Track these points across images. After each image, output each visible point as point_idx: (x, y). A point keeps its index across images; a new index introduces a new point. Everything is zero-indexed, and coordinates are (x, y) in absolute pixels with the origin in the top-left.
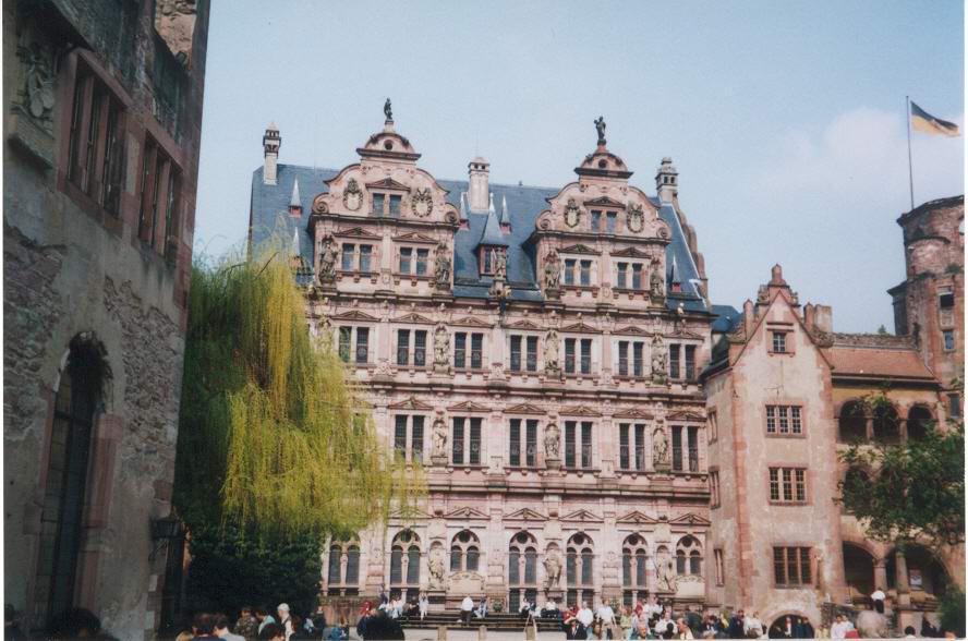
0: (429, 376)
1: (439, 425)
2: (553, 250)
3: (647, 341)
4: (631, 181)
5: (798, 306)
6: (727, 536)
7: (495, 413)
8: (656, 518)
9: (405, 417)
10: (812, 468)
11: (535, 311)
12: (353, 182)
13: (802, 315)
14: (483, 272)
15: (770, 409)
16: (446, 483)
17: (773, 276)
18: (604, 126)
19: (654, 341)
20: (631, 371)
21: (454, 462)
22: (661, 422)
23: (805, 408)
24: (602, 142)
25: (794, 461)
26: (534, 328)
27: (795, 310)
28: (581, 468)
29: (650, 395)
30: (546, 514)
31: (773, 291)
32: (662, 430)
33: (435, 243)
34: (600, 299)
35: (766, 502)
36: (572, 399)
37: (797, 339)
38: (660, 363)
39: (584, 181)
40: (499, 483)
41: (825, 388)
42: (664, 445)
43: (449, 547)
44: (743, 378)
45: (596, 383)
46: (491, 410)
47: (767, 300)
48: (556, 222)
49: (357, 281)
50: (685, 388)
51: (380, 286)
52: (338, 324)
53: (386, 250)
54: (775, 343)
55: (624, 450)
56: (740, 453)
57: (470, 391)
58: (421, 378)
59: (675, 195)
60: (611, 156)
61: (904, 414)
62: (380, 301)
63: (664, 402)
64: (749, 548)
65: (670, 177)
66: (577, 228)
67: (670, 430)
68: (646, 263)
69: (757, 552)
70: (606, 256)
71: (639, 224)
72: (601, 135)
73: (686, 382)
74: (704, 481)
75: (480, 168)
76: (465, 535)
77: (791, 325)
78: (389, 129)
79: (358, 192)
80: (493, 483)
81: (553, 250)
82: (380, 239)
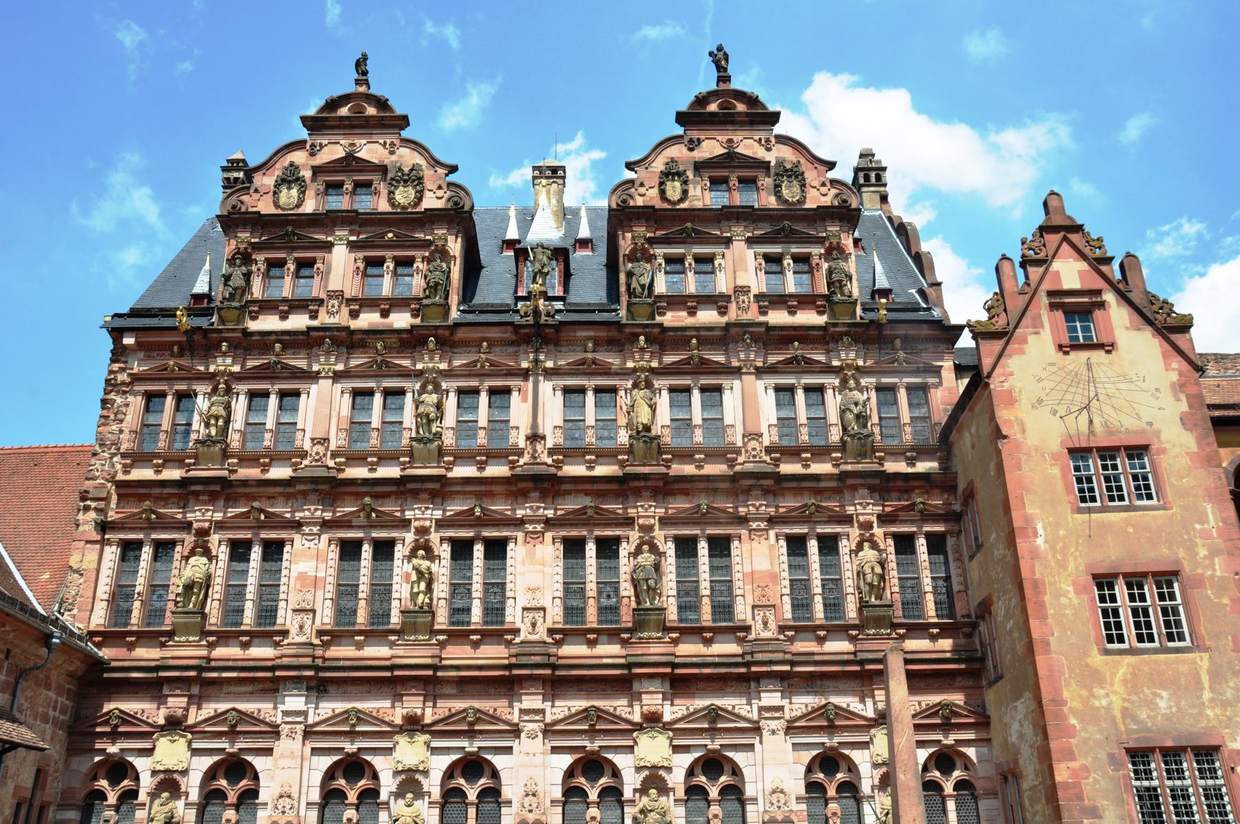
0: (404, 467)
1: (421, 552)
2: (640, 242)
3: (832, 381)
4: (778, 129)
5: (1108, 260)
6: (1021, 736)
7: (530, 528)
8: (870, 714)
9: (358, 544)
10: (1187, 568)
12: (292, 164)
13: (1118, 276)
14: (520, 294)
16: (429, 661)
17: (1047, 213)
19: (844, 382)
21: (452, 623)
22: (869, 526)
23: (1154, 448)
26: (607, 372)
27: (1104, 268)
28: (710, 624)
29: (843, 476)
30: (637, 718)
31: (1053, 239)
32: (874, 546)
33: (426, 244)
34: (733, 314)
35: (1095, 651)
36: (686, 493)
37: (1117, 315)
38: (858, 416)
39: (695, 134)
40: (537, 659)
41: (1190, 406)
42: (878, 570)
43: (436, 793)
44: (1011, 400)
45: (732, 463)
46: (520, 523)
47: (1042, 255)
48: (646, 196)
49: (284, 317)
50: (911, 462)
51: (324, 319)
52: (242, 388)
53: (340, 264)
55: (800, 588)
56: (1022, 545)
57: (483, 488)
58: (391, 471)
59: (884, 199)
60: (740, 95)
62: (319, 342)
63: (872, 489)
64: (1069, 755)
65: (873, 175)
66: (682, 206)
67: (890, 542)
68: (816, 250)
69: (1087, 762)
70: (739, 246)
71: (797, 189)
73: (912, 449)
74: (969, 636)
76: (472, 766)
77: (1098, 292)
78: (362, 89)
79: (298, 179)
80: (524, 660)
81: (640, 242)
82: (328, 246)
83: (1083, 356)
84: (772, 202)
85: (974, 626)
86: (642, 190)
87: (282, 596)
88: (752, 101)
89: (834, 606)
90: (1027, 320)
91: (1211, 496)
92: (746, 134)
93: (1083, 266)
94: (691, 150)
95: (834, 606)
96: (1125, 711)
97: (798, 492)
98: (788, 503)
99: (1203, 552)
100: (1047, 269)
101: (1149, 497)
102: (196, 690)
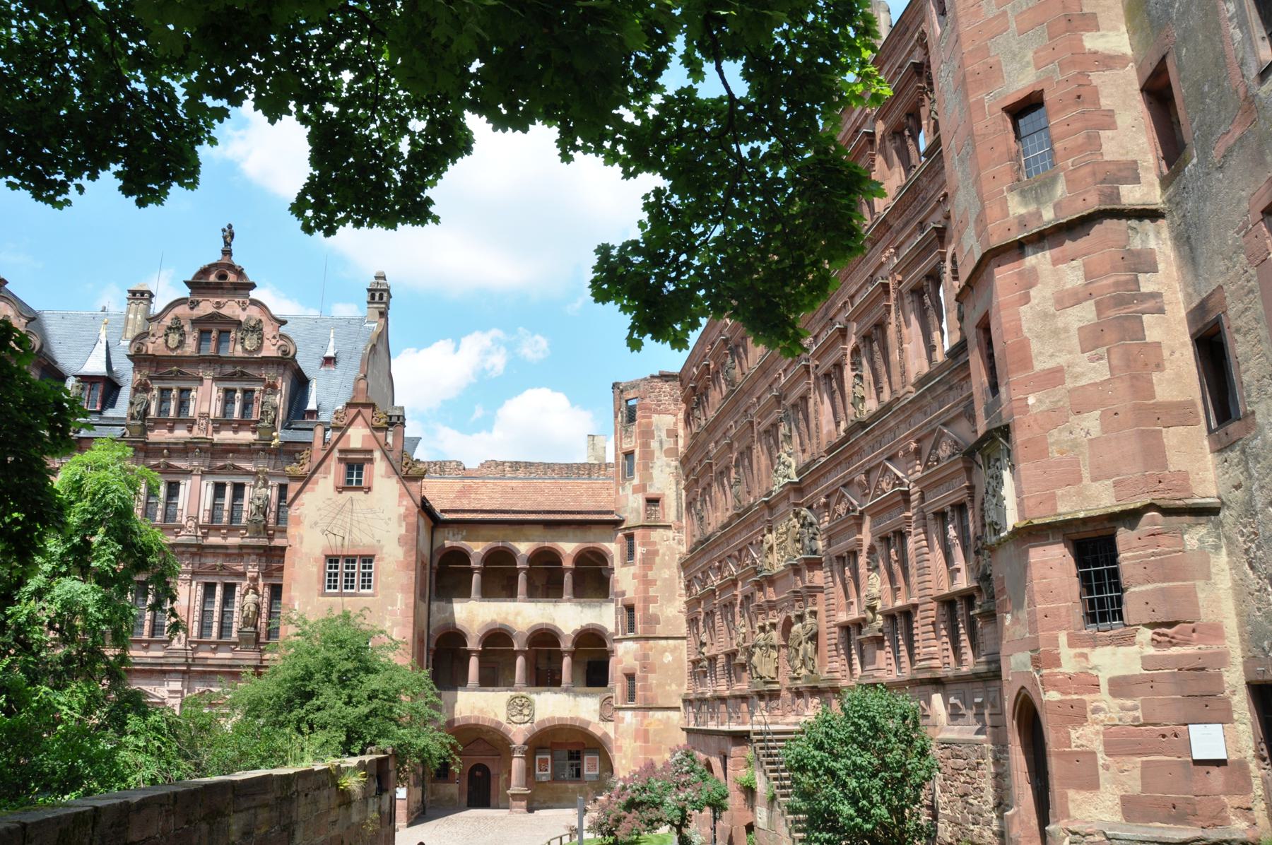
4: (254, 294)
24: (227, 252)
32: (256, 592)
34: (196, 432)
44: (298, 521)
61: (568, 563)
66: (179, 352)
68: (258, 388)
72: (227, 244)
75: (138, 295)
77: (371, 451)
86: (153, 339)
88: (240, 273)
89: (224, 628)
90: (322, 469)
91: (403, 589)
93: (367, 431)
94: (192, 309)
95: (224, 628)
97: (215, 555)
98: (209, 561)
100: (342, 435)
101: (369, 587)
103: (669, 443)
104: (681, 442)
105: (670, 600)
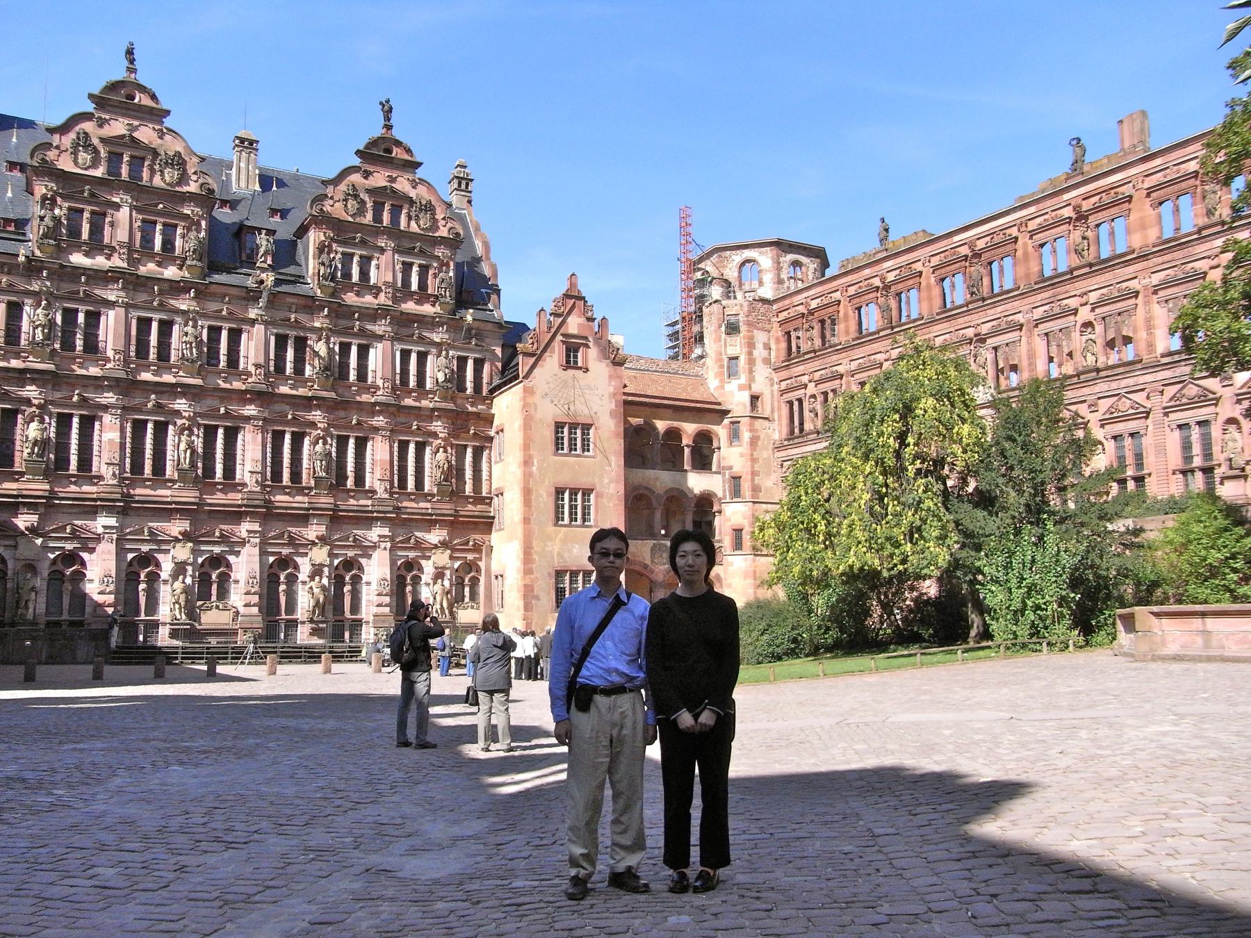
4: (420, 173)
10: (598, 488)
11: (305, 307)
15: (559, 426)
16: (193, 500)
18: (391, 108)
20: (412, 382)
25: (583, 481)
37: (593, 352)
40: (257, 502)
48: (335, 209)
54: (568, 356)
59: (470, 202)
63: (448, 418)
65: (464, 183)
66: (358, 220)
72: (387, 119)
80: (251, 503)
83: (571, 372)
84: (414, 227)
85: (491, 499)
86: (331, 202)
87: (95, 453)
92: (400, 173)
93: (582, 320)
96: (559, 554)
99: (606, 481)
102: (42, 510)
103: (765, 353)
104: (773, 354)
105: (769, 474)
